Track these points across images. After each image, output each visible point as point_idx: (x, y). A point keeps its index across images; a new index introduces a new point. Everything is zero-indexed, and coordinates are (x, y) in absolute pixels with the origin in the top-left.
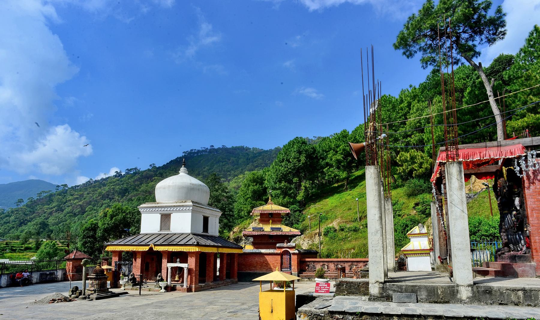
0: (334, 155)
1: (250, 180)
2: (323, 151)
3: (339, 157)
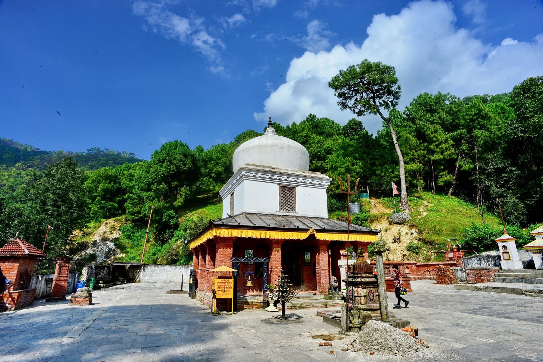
0: (215, 166)
1: (101, 177)
2: (203, 160)
3: (221, 169)
